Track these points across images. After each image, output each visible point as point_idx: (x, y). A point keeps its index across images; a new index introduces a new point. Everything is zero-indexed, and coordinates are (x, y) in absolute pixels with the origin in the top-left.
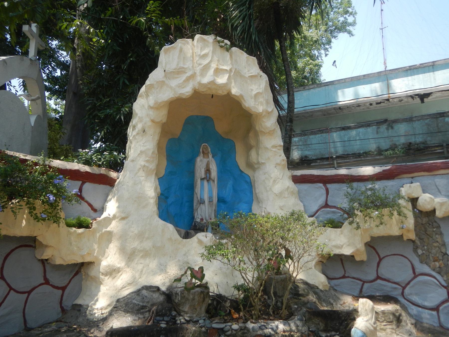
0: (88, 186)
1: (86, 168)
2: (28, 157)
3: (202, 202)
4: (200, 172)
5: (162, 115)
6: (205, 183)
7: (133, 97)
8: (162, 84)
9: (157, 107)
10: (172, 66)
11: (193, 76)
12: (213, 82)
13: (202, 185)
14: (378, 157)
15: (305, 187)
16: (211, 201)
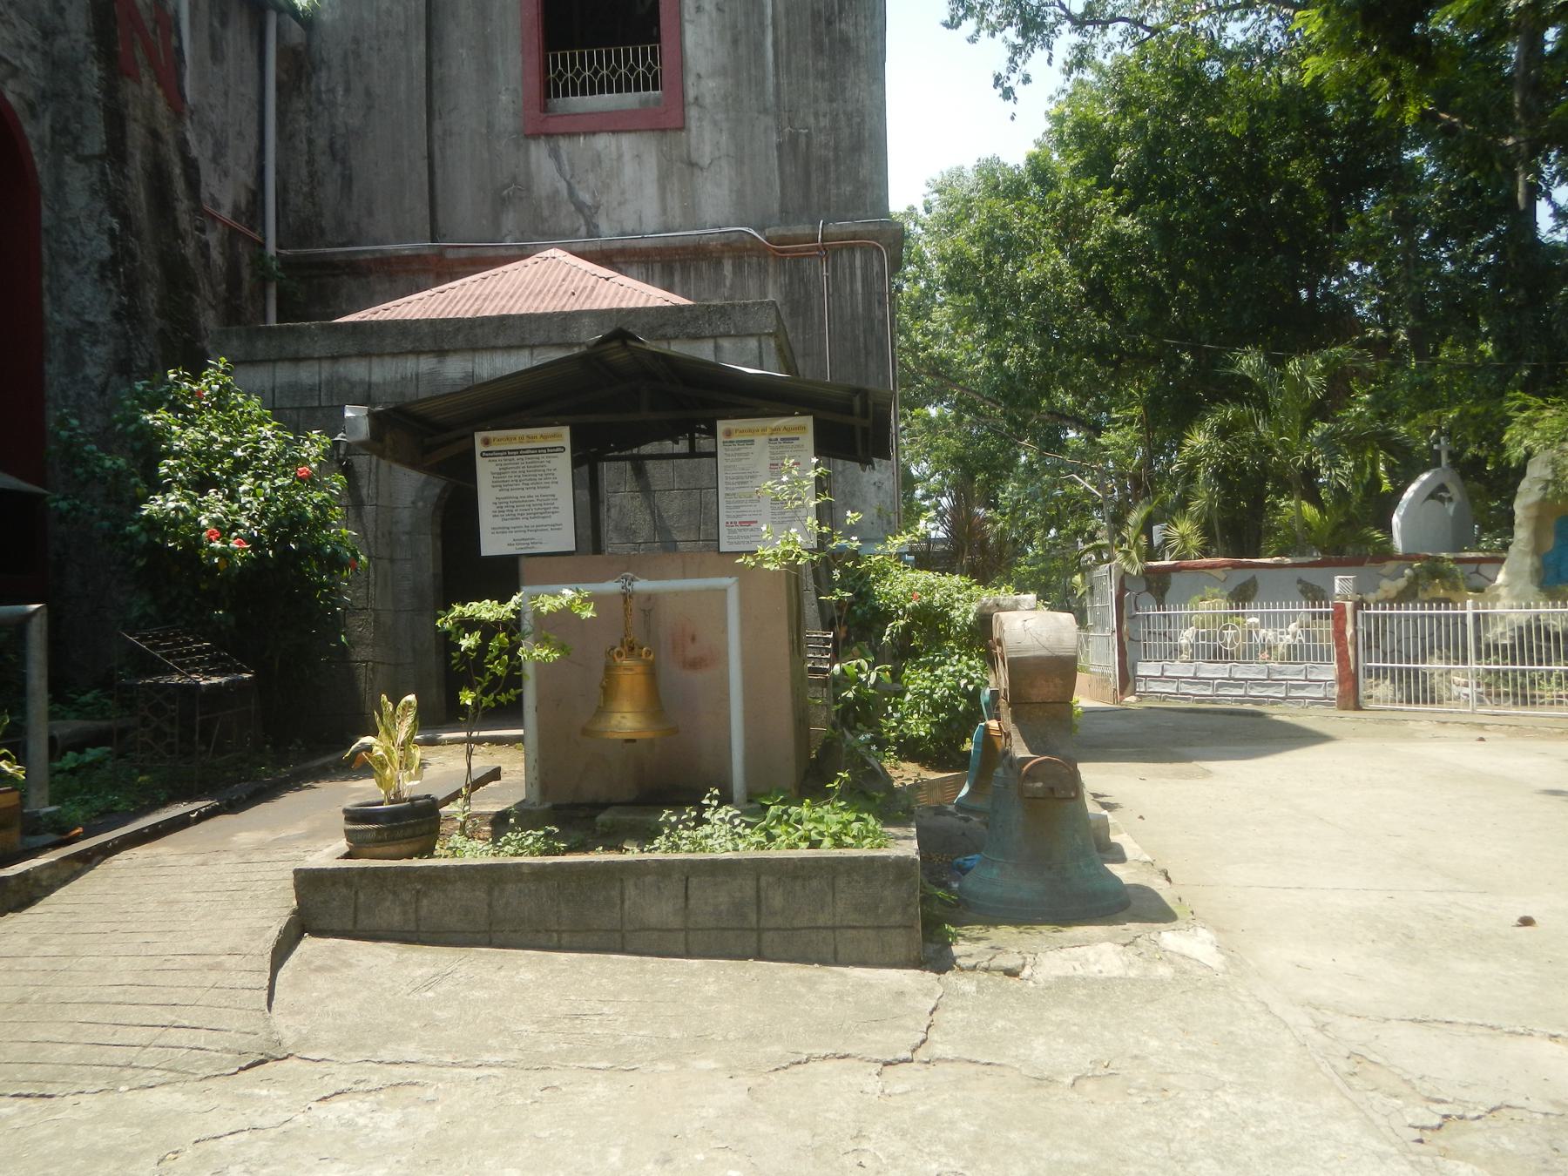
5: (1533, 512)
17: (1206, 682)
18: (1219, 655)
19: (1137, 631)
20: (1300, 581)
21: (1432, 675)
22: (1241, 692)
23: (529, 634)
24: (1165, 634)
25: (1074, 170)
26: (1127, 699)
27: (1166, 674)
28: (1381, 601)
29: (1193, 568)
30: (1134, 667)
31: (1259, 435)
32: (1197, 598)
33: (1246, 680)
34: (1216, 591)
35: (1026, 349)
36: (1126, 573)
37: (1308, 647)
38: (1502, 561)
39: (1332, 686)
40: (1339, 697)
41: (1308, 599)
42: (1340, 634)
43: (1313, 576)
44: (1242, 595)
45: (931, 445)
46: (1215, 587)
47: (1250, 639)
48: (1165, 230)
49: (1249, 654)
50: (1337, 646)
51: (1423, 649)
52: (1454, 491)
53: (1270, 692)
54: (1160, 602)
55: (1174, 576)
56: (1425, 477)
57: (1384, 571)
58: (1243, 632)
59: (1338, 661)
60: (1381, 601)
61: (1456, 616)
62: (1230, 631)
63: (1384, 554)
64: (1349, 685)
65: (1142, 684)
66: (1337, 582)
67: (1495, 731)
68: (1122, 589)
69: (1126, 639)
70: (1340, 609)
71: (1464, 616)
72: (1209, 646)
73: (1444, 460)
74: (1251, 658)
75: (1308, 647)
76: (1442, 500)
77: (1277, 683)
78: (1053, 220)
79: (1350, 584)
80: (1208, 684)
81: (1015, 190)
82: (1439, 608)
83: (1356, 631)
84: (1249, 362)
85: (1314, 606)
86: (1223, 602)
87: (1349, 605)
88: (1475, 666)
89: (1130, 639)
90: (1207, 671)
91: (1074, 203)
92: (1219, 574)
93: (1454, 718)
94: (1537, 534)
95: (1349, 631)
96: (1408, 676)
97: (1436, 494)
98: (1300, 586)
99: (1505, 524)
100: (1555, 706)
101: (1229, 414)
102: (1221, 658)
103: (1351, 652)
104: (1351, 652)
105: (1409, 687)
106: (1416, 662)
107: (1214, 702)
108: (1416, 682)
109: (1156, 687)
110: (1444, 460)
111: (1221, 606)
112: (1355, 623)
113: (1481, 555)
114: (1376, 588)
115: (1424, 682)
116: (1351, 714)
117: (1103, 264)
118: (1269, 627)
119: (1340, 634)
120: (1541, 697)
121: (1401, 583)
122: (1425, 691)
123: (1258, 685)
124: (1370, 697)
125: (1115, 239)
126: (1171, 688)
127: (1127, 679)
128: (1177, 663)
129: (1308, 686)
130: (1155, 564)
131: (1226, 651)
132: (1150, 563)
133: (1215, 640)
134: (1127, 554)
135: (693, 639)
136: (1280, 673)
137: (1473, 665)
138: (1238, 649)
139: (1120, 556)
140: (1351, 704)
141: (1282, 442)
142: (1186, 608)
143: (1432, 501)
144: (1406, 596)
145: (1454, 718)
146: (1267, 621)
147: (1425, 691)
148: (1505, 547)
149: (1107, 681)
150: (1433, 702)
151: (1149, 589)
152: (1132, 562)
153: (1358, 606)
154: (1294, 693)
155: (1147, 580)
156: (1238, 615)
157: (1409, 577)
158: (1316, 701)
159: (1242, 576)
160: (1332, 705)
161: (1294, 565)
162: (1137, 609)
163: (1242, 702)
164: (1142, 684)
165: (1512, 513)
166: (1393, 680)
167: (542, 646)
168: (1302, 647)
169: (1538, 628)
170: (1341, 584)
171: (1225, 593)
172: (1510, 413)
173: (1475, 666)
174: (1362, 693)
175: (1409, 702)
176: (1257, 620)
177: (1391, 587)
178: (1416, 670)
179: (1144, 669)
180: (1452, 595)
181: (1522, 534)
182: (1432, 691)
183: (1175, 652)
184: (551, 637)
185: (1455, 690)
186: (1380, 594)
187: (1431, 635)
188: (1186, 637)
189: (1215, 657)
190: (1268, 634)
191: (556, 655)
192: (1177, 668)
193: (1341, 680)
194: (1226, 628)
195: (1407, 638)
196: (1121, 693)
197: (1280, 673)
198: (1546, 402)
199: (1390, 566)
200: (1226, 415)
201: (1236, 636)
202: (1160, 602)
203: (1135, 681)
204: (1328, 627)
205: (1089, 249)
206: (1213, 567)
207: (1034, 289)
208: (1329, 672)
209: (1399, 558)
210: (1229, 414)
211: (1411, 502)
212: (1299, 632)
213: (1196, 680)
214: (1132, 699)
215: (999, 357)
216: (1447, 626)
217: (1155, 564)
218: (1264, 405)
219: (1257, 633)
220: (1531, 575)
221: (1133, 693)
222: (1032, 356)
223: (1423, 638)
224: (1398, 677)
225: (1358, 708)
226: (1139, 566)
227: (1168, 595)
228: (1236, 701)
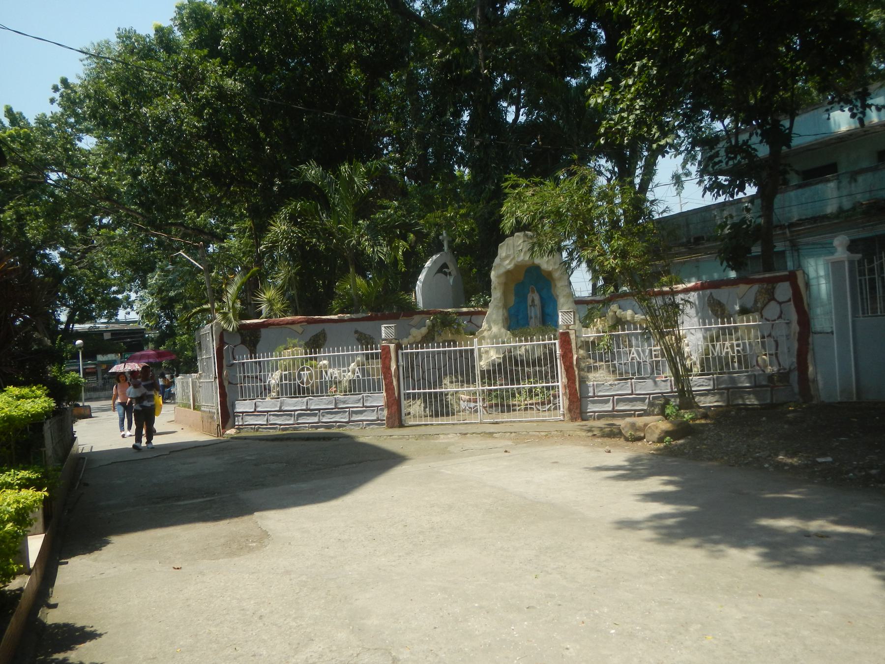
0: (474, 317)
1: (472, 309)
2: (450, 310)
3: (531, 318)
4: (529, 302)
5: (503, 279)
6: (532, 308)
7: (490, 269)
8: (500, 265)
9: (498, 277)
10: (504, 255)
11: (514, 258)
12: (523, 260)
13: (531, 309)
14: (836, 221)
15: (580, 306)
16: (536, 317)
17: (289, 413)
18: (299, 391)
19: (235, 376)
20: (356, 332)
22: (316, 419)
24: (257, 377)
25: (192, 45)
26: (228, 432)
27: (258, 409)
28: (420, 342)
29: (278, 324)
30: (233, 406)
31: (323, 224)
32: (281, 347)
33: (319, 410)
34: (296, 341)
35: (155, 168)
36: (224, 330)
37: (364, 380)
38: (484, 313)
39: (382, 410)
40: (387, 418)
42: (386, 369)
43: (365, 327)
44: (315, 344)
45: (111, 253)
46: (295, 338)
47: (321, 378)
48: (257, 88)
49: (322, 389)
52: (452, 268)
53: (337, 418)
54: (253, 352)
55: (263, 331)
56: (434, 257)
57: (412, 323)
58: (316, 372)
59: (386, 391)
60: (420, 342)
61: (466, 351)
62: (306, 372)
63: (410, 310)
64: (395, 407)
65: (240, 418)
66: (383, 329)
67: (501, 438)
68: (221, 343)
69: (226, 384)
70: (386, 350)
71: (472, 351)
72: (290, 384)
73: (446, 248)
74: (322, 392)
75: (364, 380)
76: (446, 274)
77: (342, 411)
78: (175, 76)
79: (393, 331)
80: (291, 415)
81: (147, 53)
82: (449, 346)
83: (398, 367)
84: (312, 172)
86: (301, 350)
87: (392, 346)
88: (481, 388)
89: (230, 383)
90: (289, 405)
91: (189, 64)
92: (298, 328)
93: (473, 429)
94: (505, 294)
95: (393, 367)
97: (442, 269)
98: (356, 335)
99: (486, 287)
100: (529, 411)
101: (299, 205)
102: (299, 393)
103: (395, 383)
104: (395, 383)
107: (295, 429)
108: (436, 401)
109: (250, 420)
110: (446, 248)
111: (299, 353)
112: (397, 361)
113: (472, 309)
114: (408, 335)
115: (441, 400)
116: (397, 432)
117: (213, 109)
118: (335, 367)
119: (386, 369)
120: (514, 405)
121: (424, 330)
122: (442, 405)
123: (328, 413)
124: (409, 414)
125: (221, 93)
126: (261, 421)
127: (227, 415)
128: (268, 399)
129: (365, 411)
130: (248, 322)
131: (303, 388)
132: (244, 322)
133: (295, 380)
134: (225, 315)
137: (478, 387)
138: (312, 386)
139: (218, 316)
140: (397, 423)
141: (340, 229)
142: (272, 356)
143: (440, 275)
144: (428, 339)
145: (473, 429)
146: (335, 362)
147: (442, 405)
148: (486, 304)
149: (212, 417)
150: (448, 415)
151: (243, 342)
152: (228, 321)
153: (399, 347)
154: (355, 418)
155: (242, 335)
156: (311, 359)
157: (429, 326)
158: (371, 422)
159: (315, 329)
160: (383, 424)
161: (351, 320)
162: (234, 359)
163: (317, 427)
164: (240, 418)
165: (490, 281)
166: (425, 401)
168: (359, 381)
169: (510, 358)
170: (386, 330)
171: (303, 343)
172: (507, 191)
173: (481, 388)
174: (404, 411)
176: (325, 362)
177: (418, 333)
178: (436, 393)
179: (242, 406)
180: (455, 337)
181: (496, 294)
182: (447, 407)
183: (266, 390)
185: (463, 405)
186: (411, 339)
187: (445, 366)
188: (274, 379)
189: (295, 394)
190: (335, 372)
192: (268, 404)
193: (389, 405)
194: (303, 370)
195: (429, 370)
196: (224, 427)
197: (344, 402)
198: (530, 181)
199: (417, 318)
200: (296, 206)
201: (311, 375)
202: (253, 352)
203: (234, 417)
204: (377, 365)
205: (202, 98)
206: (293, 323)
207: (160, 122)
208: (379, 399)
209: (422, 312)
210: (299, 205)
212: (357, 369)
213: (281, 412)
214: (231, 432)
215: (135, 174)
216: (456, 360)
217: (248, 322)
218: (328, 207)
219: (326, 373)
220: (503, 322)
221: (233, 426)
222: (160, 173)
223: (439, 369)
224: (425, 397)
225: (401, 425)
226: (234, 324)
227: (258, 347)
228: (312, 427)
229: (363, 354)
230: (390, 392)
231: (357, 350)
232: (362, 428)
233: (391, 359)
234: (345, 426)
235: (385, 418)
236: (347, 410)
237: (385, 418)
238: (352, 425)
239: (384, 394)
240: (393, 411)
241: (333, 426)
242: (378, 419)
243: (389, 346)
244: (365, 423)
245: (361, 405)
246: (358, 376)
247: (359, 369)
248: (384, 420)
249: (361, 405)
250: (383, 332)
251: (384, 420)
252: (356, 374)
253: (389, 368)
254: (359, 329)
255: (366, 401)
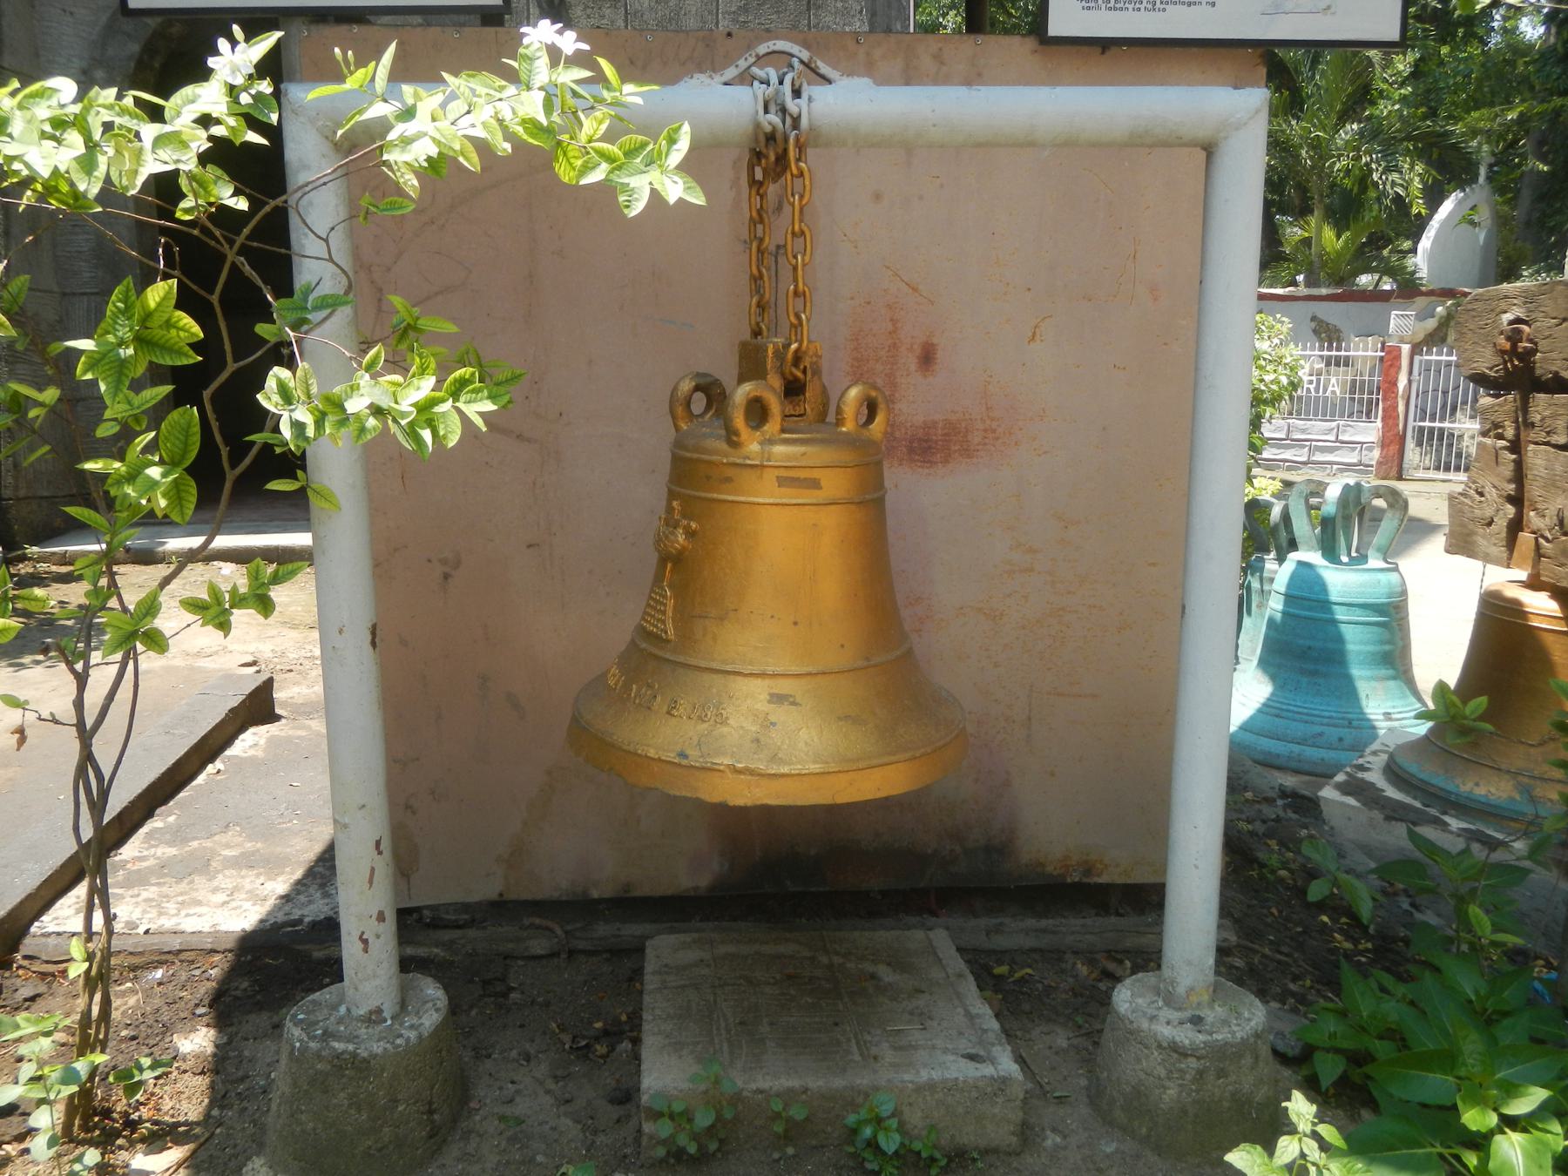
21: (1461, 437)
23: (330, 304)
39: (1370, 449)
40: (1380, 463)
41: (1321, 340)
50: (1385, 399)
51: (1444, 406)
53: (1288, 455)
64: (1394, 448)
66: (1393, 316)
83: (1410, 382)
85: (1330, 348)
87: (1406, 348)
95: (1402, 382)
96: (1441, 439)
98: (1313, 325)
103: (1401, 408)
104: (1401, 408)
105: (1439, 452)
106: (1433, 419)
112: (1410, 373)
115: (1450, 445)
122: (1449, 454)
135: (927, 358)
136: (1303, 431)
140: (1394, 472)
143: (1465, 226)
157: (1441, 317)
160: (1371, 472)
167: (397, 364)
175: (1438, 468)
178: (1441, 430)
184: (429, 324)
191: (478, 408)
193: (1384, 444)
197: (1303, 431)
211: (1444, 223)
223: (1445, 393)
229: (1321, 357)
230: (1391, 422)
231: (1313, 349)
232: (1329, 475)
233: (1399, 368)
234: (1300, 469)
235: (1374, 463)
236: (1308, 443)
237: (1374, 463)
238: (1313, 468)
239: (1379, 424)
240: (1391, 453)
241: (1279, 467)
242: (1360, 464)
243: (1399, 349)
244: (1335, 467)
245: (1333, 439)
246: (1333, 392)
247: (1338, 380)
248: (1372, 466)
249: (1333, 439)
250: (1392, 321)
251: (1372, 466)
252: (1330, 389)
253: (1394, 384)
254: (1320, 315)
255: (1345, 431)
